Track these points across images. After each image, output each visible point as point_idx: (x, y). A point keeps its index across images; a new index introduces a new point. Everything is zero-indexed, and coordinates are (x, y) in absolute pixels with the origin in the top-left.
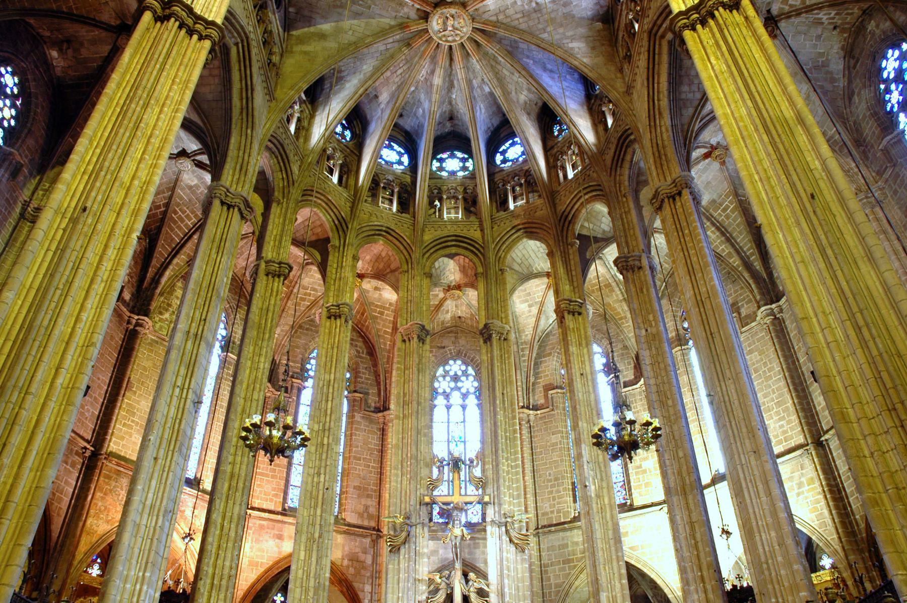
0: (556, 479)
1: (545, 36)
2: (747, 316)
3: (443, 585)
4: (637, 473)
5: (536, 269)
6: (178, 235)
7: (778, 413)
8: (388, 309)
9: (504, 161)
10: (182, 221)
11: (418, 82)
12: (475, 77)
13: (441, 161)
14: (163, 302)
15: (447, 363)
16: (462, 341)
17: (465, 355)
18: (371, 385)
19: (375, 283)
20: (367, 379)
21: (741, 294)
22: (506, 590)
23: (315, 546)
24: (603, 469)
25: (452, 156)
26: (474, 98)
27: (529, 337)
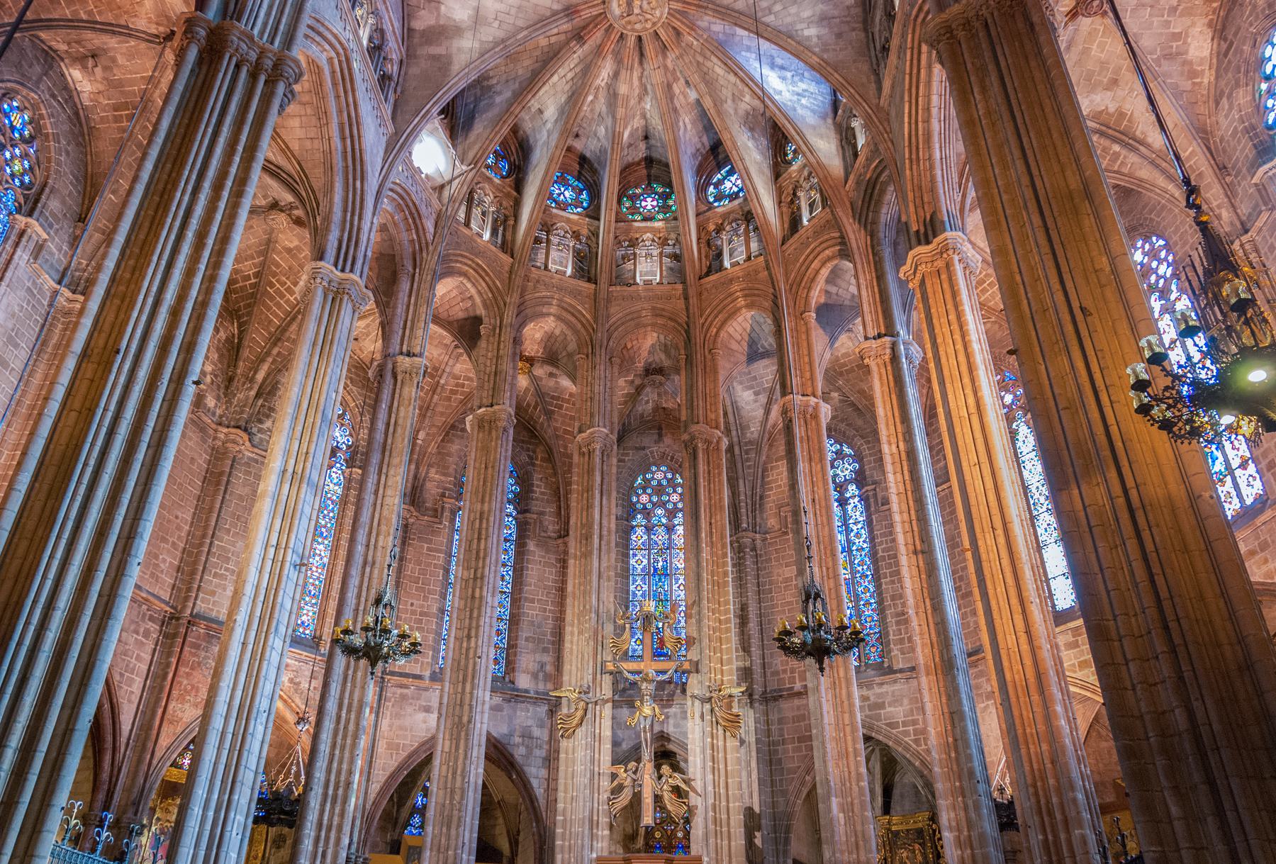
1: (770, 19)
3: (628, 782)
4: (898, 623)
5: (763, 347)
6: (276, 316)
8: (568, 401)
9: (719, 198)
10: (282, 296)
11: (598, 89)
12: (676, 79)
13: (633, 198)
14: (262, 406)
17: (672, 458)
19: (549, 369)
20: (542, 493)
25: (650, 191)
26: (675, 110)
27: (756, 435)
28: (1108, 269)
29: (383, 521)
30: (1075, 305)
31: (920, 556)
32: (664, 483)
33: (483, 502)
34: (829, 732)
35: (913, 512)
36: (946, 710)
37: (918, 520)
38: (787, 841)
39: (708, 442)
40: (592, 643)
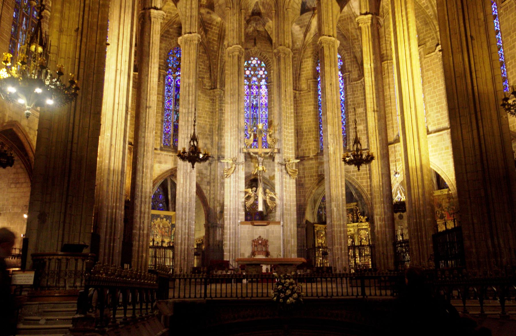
0: (309, 131)
2: (430, 48)
3: (253, 195)
5: (307, 7)
7: (437, 109)
8: (215, 26)
15: (249, 59)
16: (259, 45)
17: (260, 54)
18: (206, 72)
19: (207, 10)
20: (203, 69)
21: (429, 33)
22: (284, 198)
23: (188, 177)
24: (338, 138)
27: (299, 46)
28: (483, 19)
29: (151, 89)
30: (469, 34)
31: (376, 113)
32: (257, 65)
33: (189, 78)
34: (333, 178)
35: (374, 94)
36: (380, 173)
37: (376, 98)
38: (304, 214)
39: (285, 53)
40: (237, 140)
